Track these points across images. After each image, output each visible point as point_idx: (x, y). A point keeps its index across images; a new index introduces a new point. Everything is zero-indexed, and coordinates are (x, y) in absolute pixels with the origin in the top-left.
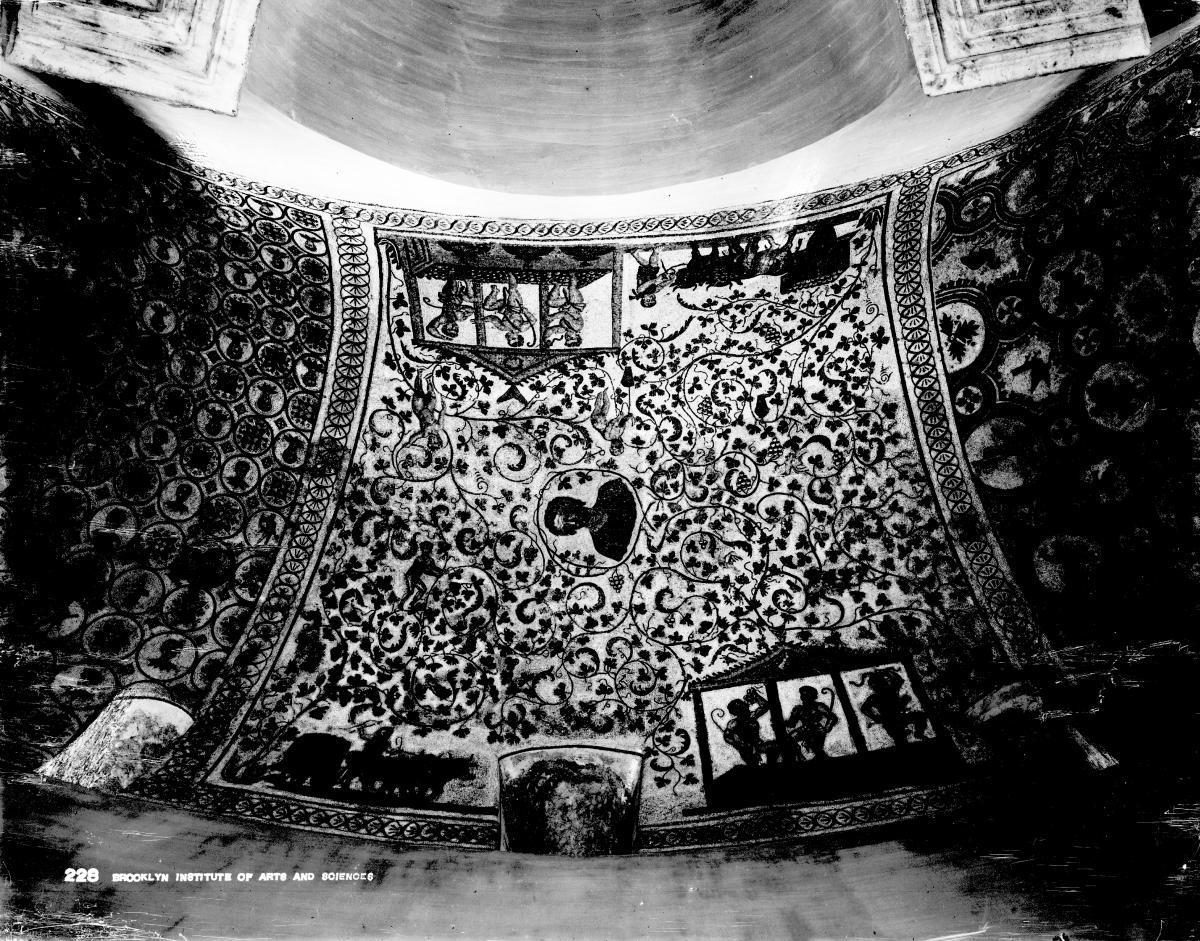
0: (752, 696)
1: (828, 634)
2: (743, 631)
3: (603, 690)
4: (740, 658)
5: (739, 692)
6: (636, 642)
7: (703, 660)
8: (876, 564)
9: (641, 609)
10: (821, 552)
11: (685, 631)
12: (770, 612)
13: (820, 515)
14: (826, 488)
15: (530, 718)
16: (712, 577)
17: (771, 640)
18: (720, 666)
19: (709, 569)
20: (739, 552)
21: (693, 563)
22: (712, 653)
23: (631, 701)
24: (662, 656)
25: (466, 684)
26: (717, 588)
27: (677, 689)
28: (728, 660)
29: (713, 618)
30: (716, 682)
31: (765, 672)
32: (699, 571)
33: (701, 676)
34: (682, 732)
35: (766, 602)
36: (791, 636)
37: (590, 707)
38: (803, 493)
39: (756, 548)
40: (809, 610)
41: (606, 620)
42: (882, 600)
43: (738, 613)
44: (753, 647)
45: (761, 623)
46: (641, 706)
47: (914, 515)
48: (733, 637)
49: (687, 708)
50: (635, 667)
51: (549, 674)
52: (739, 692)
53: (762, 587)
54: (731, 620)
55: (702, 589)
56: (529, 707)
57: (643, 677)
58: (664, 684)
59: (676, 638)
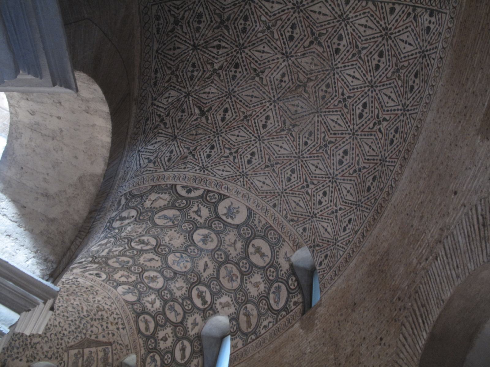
0: (79, 352)
1: (95, 336)
2: (77, 334)
3: (50, 347)
4: (77, 342)
5: (76, 351)
6: (56, 335)
7: (70, 341)
8: (105, 317)
9: (56, 326)
10: (92, 314)
11: (66, 333)
12: (83, 329)
13: (90, 305)
14: (87, 300)
15: (35, 355)
16: (70, 319)
17: (84, 337)
18: (73, 343)
19: (68, 317)
20: (74, 313)
21: (64, 316)
22: (71, 339)
23: (56, 350)
24: (62, 339)
25: (22, 346)
26: (70, 322)
27: (64, 349)
28: (74, 341)
29: (71, 330)
30: (72, 347)
31: (82, 345)
32: (66, 318)
33: (69, 345)
34: (64, 362)
35: (82, 326)
36: (88, 336)
37: (47, 352)
38: (82, 301)
39: (77, 313)
40: (91, 329)
41: (49, 328)
42: (107, 327)
43: (76, 328)
44: (79, 338)
45: (80, 332)
46: (58, 352)
47: (110, 306)
48: (75, 335)
49: (66, 354)
50: (56, 342)
51: (38, 343)
52: (76, 351)
53: (80, 322)
54: (75, 331)
55: (67, 322)
56: (35, 352)
57: (58, 345)
58: (61, 347)
59: (64, 334)
